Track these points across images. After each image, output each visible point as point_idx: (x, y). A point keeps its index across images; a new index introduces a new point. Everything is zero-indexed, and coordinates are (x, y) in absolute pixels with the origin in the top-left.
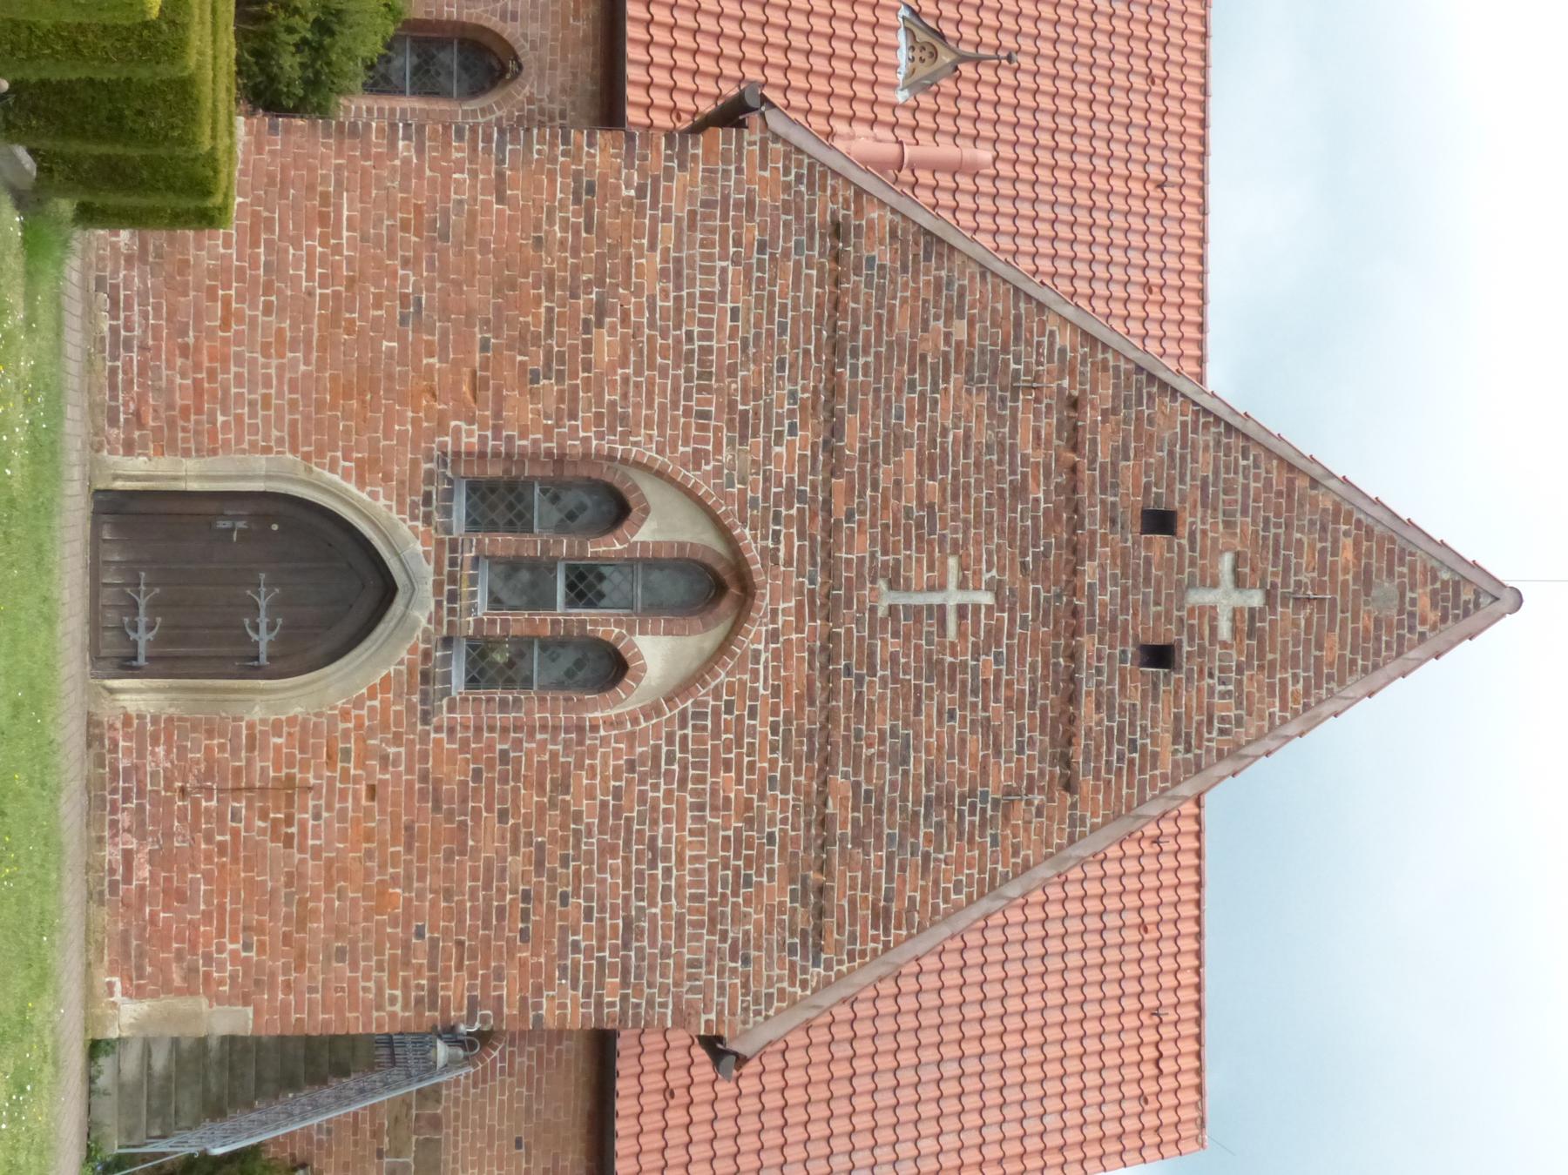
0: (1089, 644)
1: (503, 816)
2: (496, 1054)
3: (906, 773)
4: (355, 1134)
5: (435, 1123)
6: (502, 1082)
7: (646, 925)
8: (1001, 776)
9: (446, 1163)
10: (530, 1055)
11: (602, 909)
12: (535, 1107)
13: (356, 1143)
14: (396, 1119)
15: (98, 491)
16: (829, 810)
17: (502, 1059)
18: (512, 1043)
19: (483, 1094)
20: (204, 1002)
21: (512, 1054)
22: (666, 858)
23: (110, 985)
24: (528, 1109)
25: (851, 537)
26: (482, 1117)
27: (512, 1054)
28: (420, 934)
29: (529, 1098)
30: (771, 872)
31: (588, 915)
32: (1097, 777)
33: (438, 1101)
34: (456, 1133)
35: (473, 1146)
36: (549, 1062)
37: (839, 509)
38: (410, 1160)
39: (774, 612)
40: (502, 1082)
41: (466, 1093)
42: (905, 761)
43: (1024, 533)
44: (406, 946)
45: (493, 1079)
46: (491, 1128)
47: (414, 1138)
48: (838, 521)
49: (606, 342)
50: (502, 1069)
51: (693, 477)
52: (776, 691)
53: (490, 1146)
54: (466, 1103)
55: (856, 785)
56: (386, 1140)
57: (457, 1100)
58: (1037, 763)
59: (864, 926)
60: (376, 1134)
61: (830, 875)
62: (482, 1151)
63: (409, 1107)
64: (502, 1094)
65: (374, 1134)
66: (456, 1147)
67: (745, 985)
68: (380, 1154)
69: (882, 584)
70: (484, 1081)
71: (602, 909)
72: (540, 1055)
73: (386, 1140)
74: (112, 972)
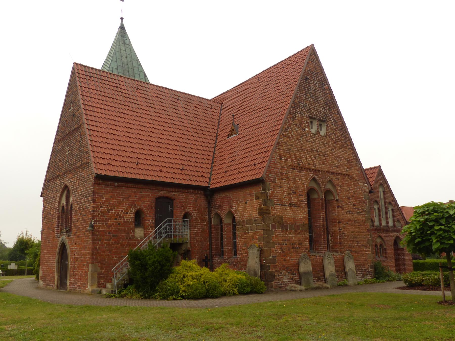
0: (72, 129)
1: (77, 221)
2: (233, 210)
3: (78, 154)
4: (245, 238)
5: (243, 221)
6: (237, 208)
7: (118, 191)
8: (79, 138)
9: (249, 218)
10: (233, 203)
11: (84, 202)
12: (241, 200)
13: (247, 238)
14: (243, 230)
15: (58, 288)
16: (79, 166)
17: (233, 209)
18: (231, 207)
19: (239, 212)
20: (88, 273)
21: (233, 207)
22: (81, 192)
23: (87, 290)
24: (241, 202)
25: (63, 171)
26: (242, 211)
27: (233, 207)
28: (85, 234)
29: (239, 202)
30: (83, 173)
31: (85, 204)
32: (80, 122)
33: (240, 221)
34: (245, 217)
35: (247, 213)
36: (234, 199)
37: (61, 174)
38: (249, 226)
39: (67, 181)
40: (237, 208)
41: (239, 215)
42: (77, 154)
43: (65, 144)
44: (86, 236)
45: (236, 210)
46: (244, 209)
47: (246, 226)
48: (62, 173)
49: (52, 213)
50: (235, 208)
51: (59, 197)
52: (71, 178)
53: (247, 209)
54: (240, 215)
55: (78, 162)
56: (246, 232)
57: (240, 217)
58: (78, 133)
59: (88, 155)
60: (245, 234)
61: (83, 164)
62: (247, 211)
63: (241, 227)
64: (239, 208)
65: (245, 234)
66: (247, 216)
67: (91, 174)
68: (248, 233)
69: (67, 164)
70: (237, 212)
71: (84, 202)
72: (233, 201)
73: (246, 232)
74: (85, 289)
